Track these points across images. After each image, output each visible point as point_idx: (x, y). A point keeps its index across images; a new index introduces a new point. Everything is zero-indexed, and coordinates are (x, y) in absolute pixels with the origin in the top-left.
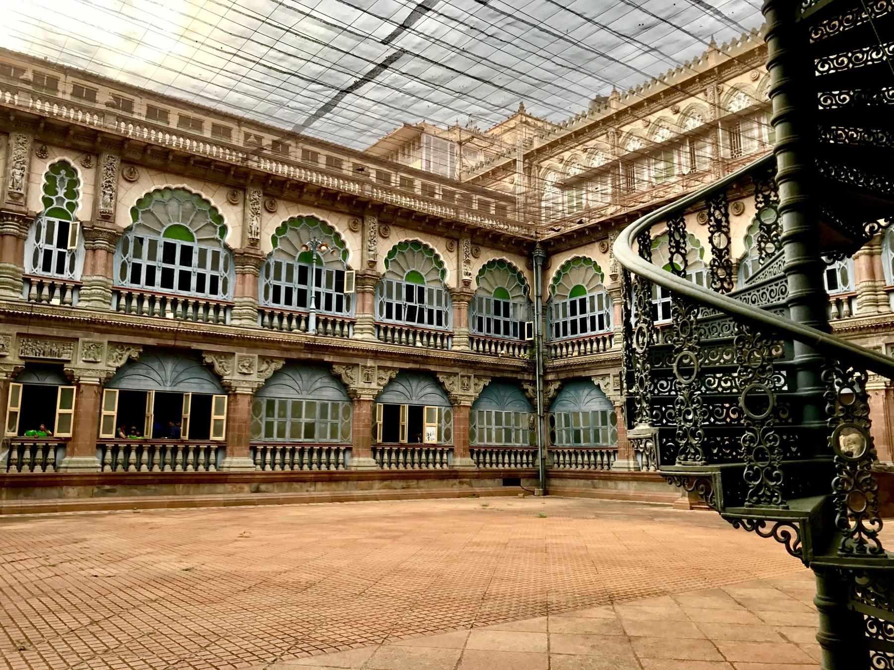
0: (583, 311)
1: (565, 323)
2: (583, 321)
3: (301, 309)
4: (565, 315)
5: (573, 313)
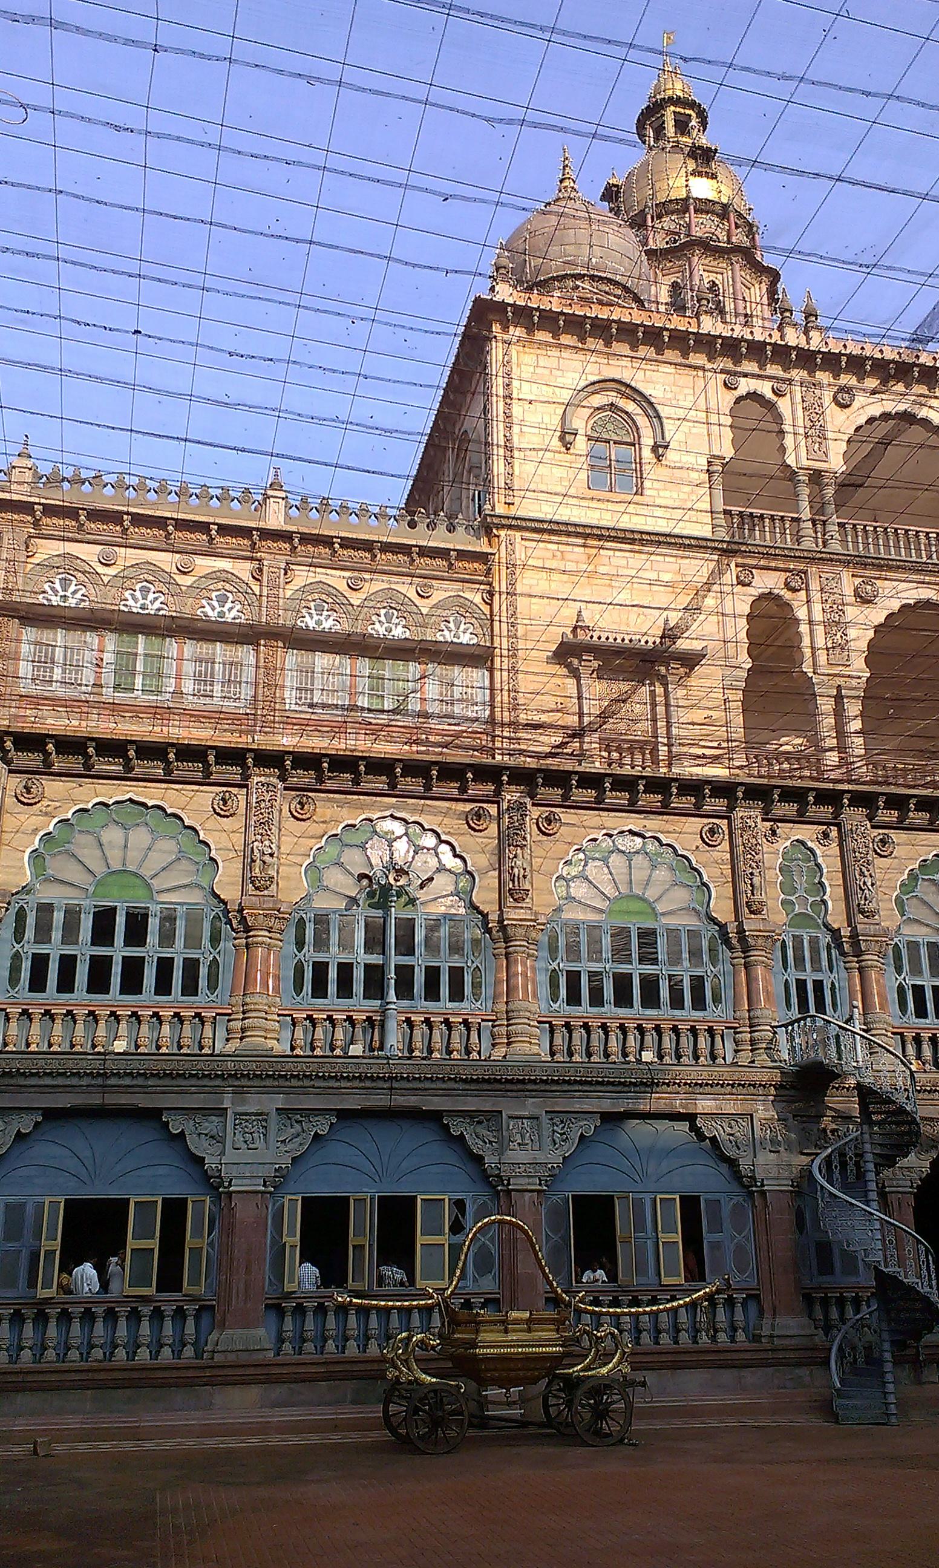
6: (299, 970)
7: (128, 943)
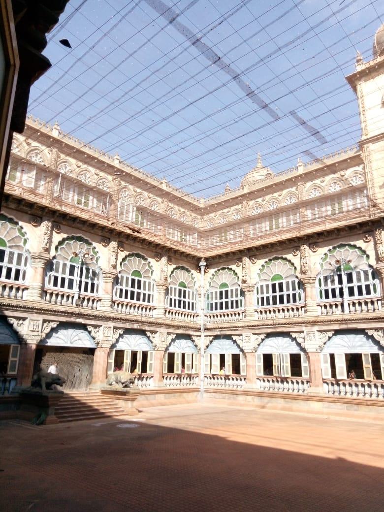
0: (227, 297)
1: (216, 304)
2: (227, 303)
3: (70, 291)
4: (216, 298)
5: (221, 298)
6: (321, 292)
7: (279, 292)
